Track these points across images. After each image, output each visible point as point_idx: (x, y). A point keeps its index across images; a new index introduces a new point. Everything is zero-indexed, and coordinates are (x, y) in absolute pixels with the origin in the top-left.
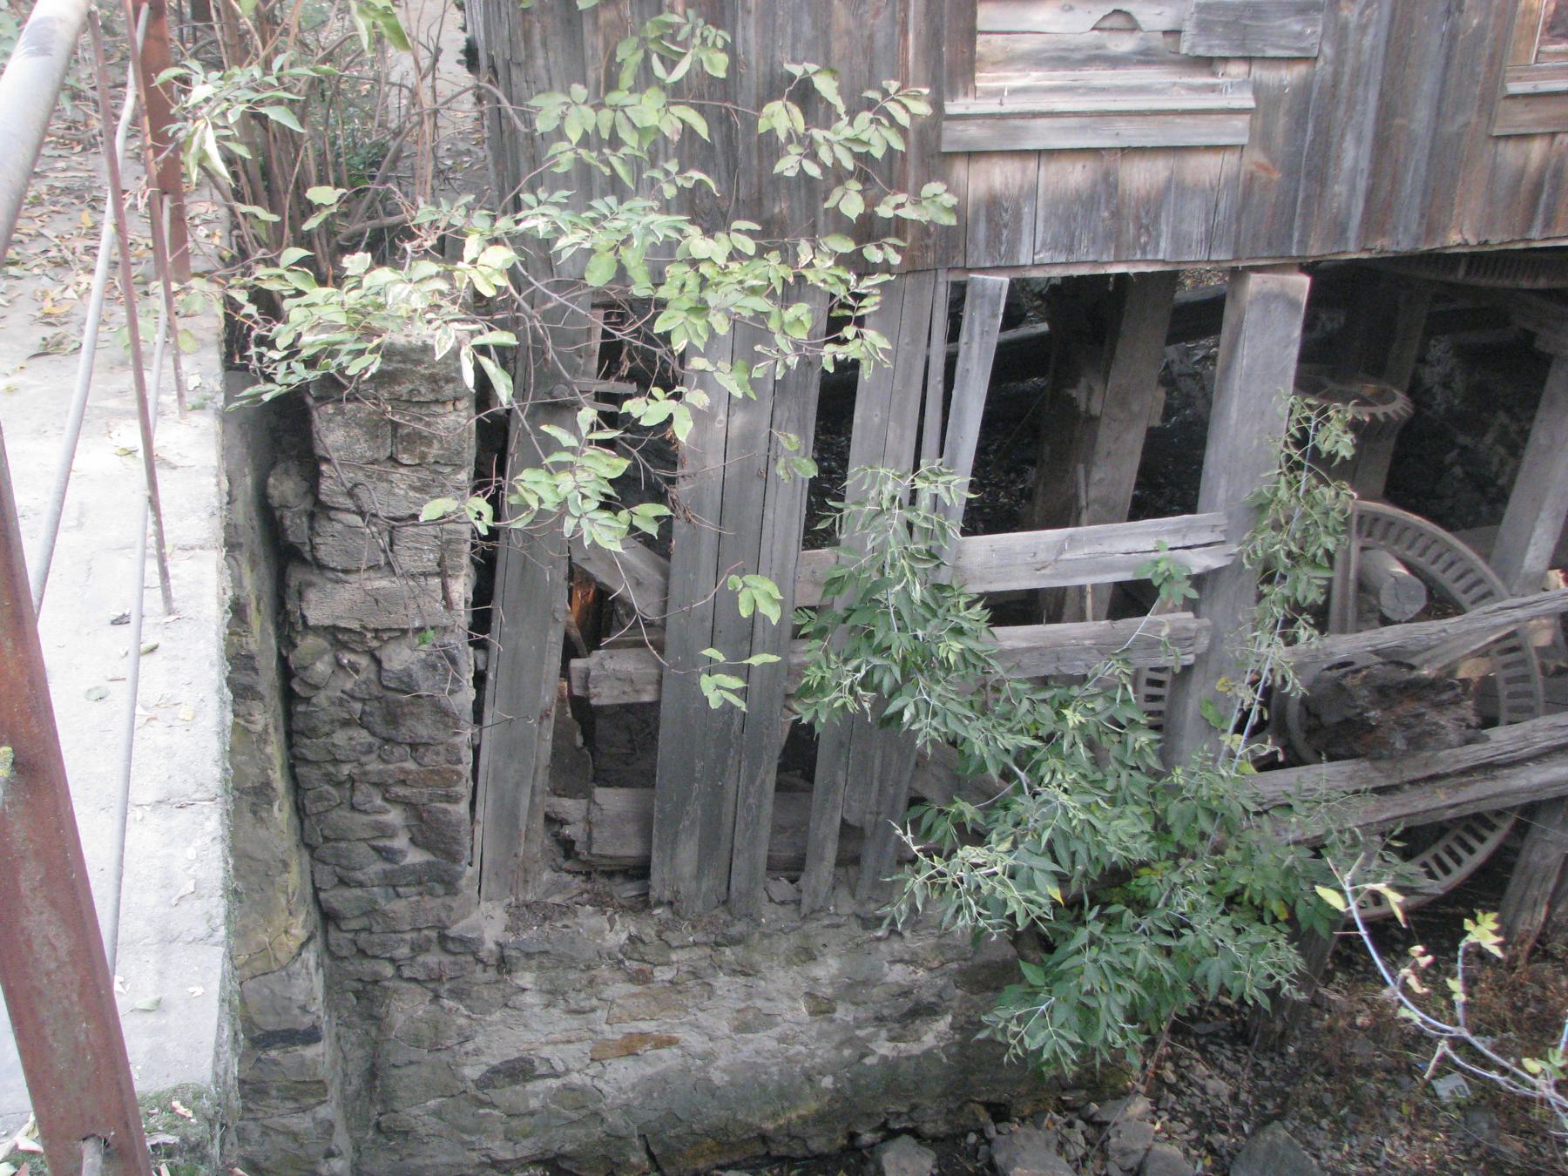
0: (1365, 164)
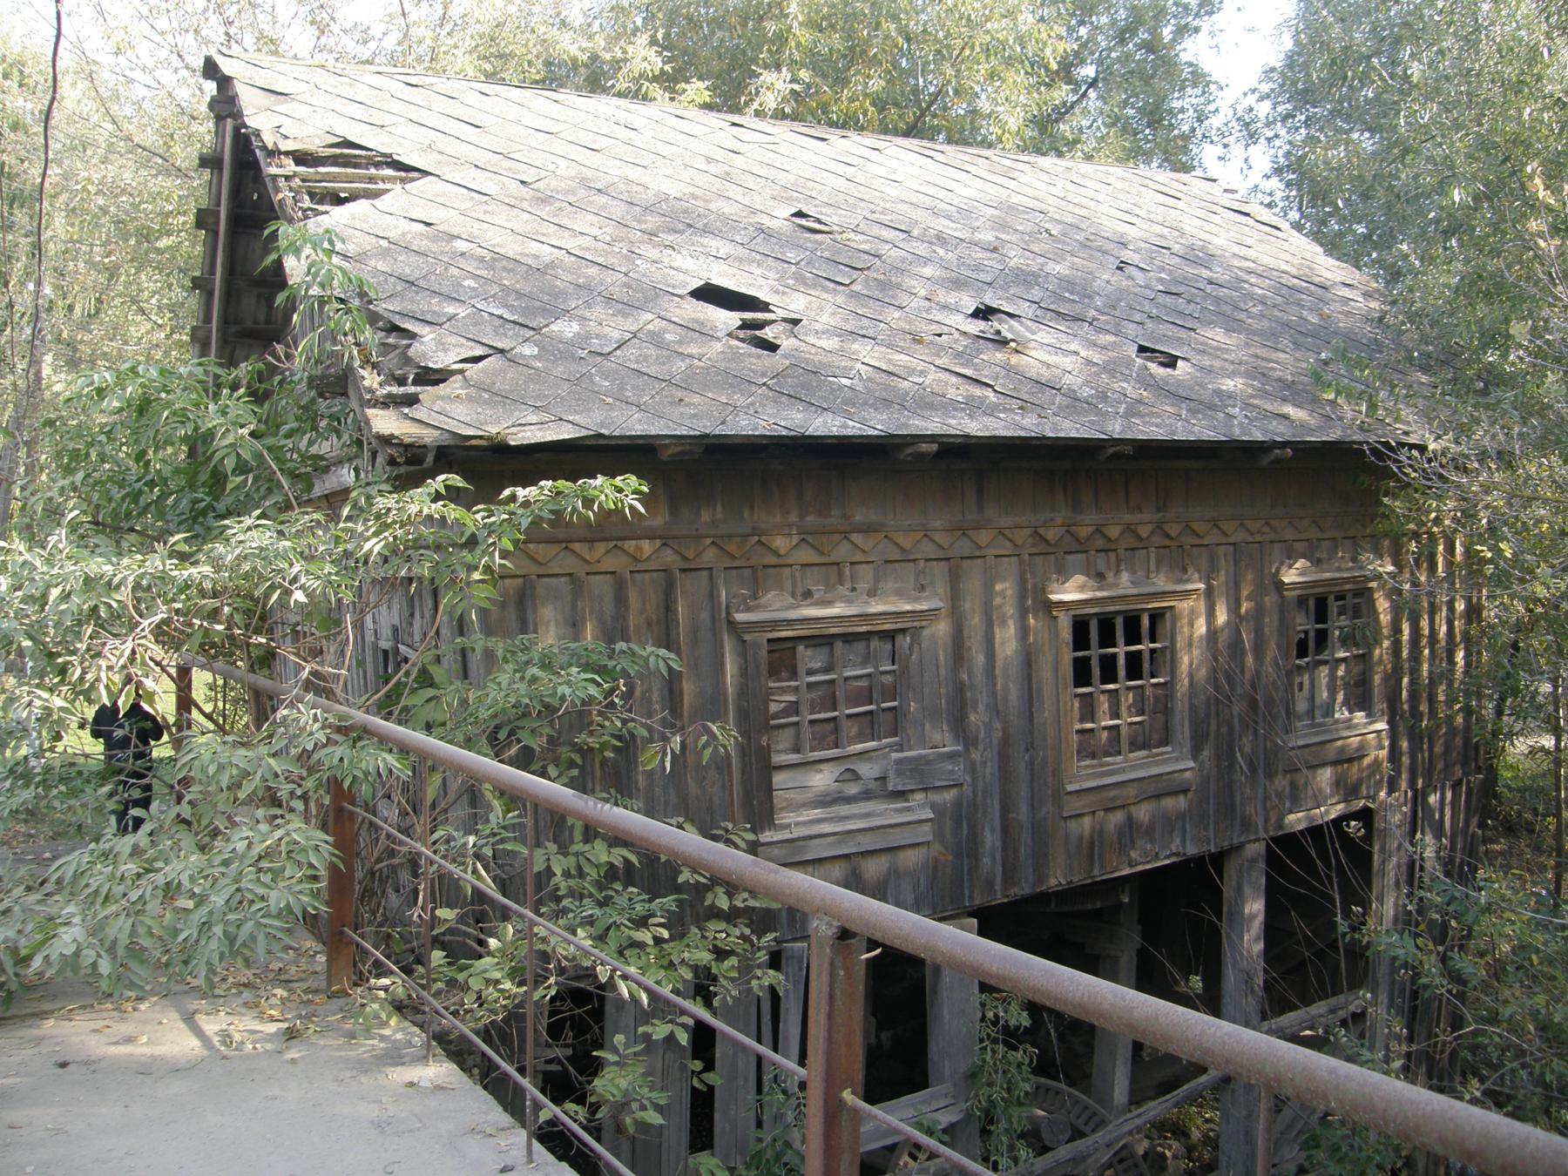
0: (998, 844)
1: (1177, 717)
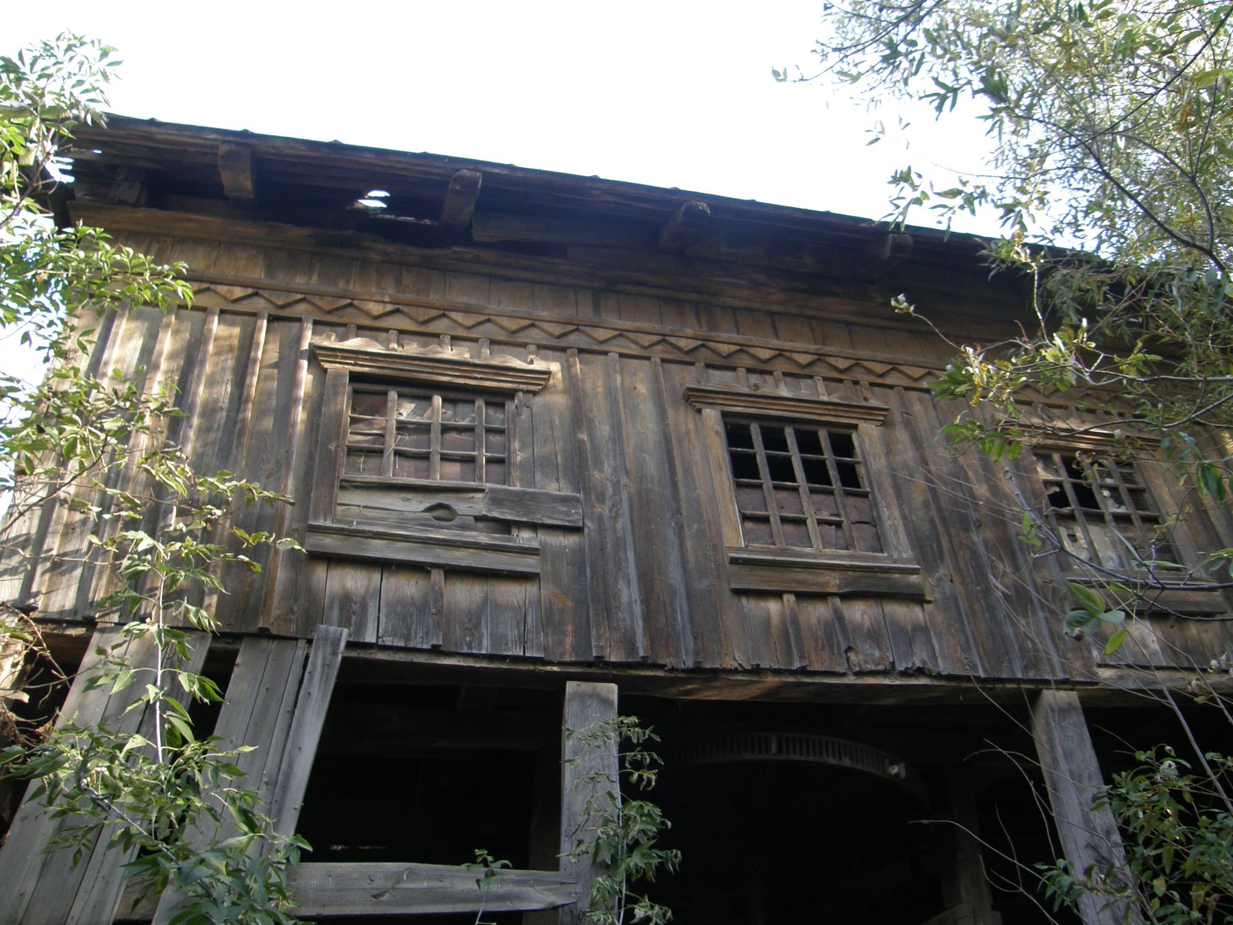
0: (636, 596)
1: (888, 523)
